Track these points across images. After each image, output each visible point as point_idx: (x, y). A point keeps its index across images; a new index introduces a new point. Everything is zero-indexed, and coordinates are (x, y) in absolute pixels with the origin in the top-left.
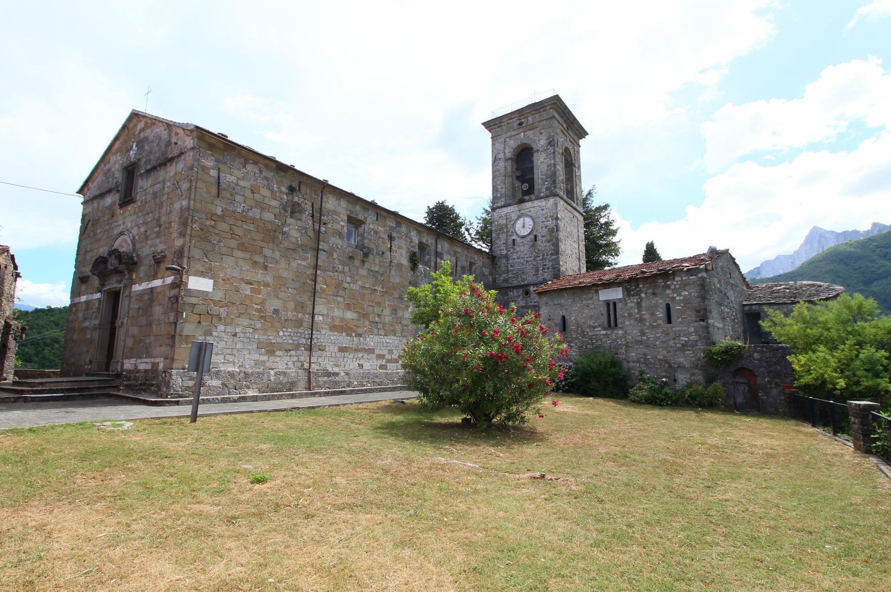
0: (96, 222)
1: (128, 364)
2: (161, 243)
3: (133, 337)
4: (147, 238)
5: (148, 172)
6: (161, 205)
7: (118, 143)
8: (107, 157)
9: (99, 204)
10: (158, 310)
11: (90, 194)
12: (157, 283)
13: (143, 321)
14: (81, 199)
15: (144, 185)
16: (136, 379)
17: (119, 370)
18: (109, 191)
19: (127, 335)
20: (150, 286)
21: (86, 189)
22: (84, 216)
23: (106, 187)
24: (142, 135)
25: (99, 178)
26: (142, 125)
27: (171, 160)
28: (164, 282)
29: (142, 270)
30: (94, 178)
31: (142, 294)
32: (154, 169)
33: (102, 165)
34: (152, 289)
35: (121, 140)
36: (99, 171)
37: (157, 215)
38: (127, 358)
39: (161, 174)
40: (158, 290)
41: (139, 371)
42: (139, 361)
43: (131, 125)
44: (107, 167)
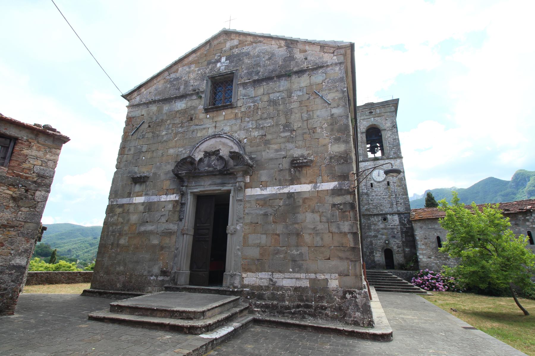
0: (155, 125)
1: (252, 279)
2: (296, 147)
3: (259, 245)
4: (267, 143)
5: (257, 83)
6: (288, 113)
7: (194, 55)
8: (175, 68)
9: (160, 110)
10: (308, 218)
11: (137, 99)
12: (305, 188)
13: (280, 228)
14: (127, 103)
15: (241, 95)
16: (282, 298)
17: (237, 283)
18: (183, 97)
19: (245, 243)
20: (286, 190)
21: (136, 94)
22: (129, 120)
23: (173, 93)
24: (236, 51)
25: (160, 85)
26: (235, 42)
27: (300, 72)
28: (315, 187)
29: (264, 175)
30: (149, 85)
31: (265, 201)
32: (269, 79)
33: (166, 73)
34: (290, 195)
35: (198, 54)
36: (159, 79)
37: (283, 120)
38: (246, 270)
39: (284, 84)
40: (307, 196)
41: (282, 288)
42: (276, 275)
43: (216, 42)
44: (173, 76)
